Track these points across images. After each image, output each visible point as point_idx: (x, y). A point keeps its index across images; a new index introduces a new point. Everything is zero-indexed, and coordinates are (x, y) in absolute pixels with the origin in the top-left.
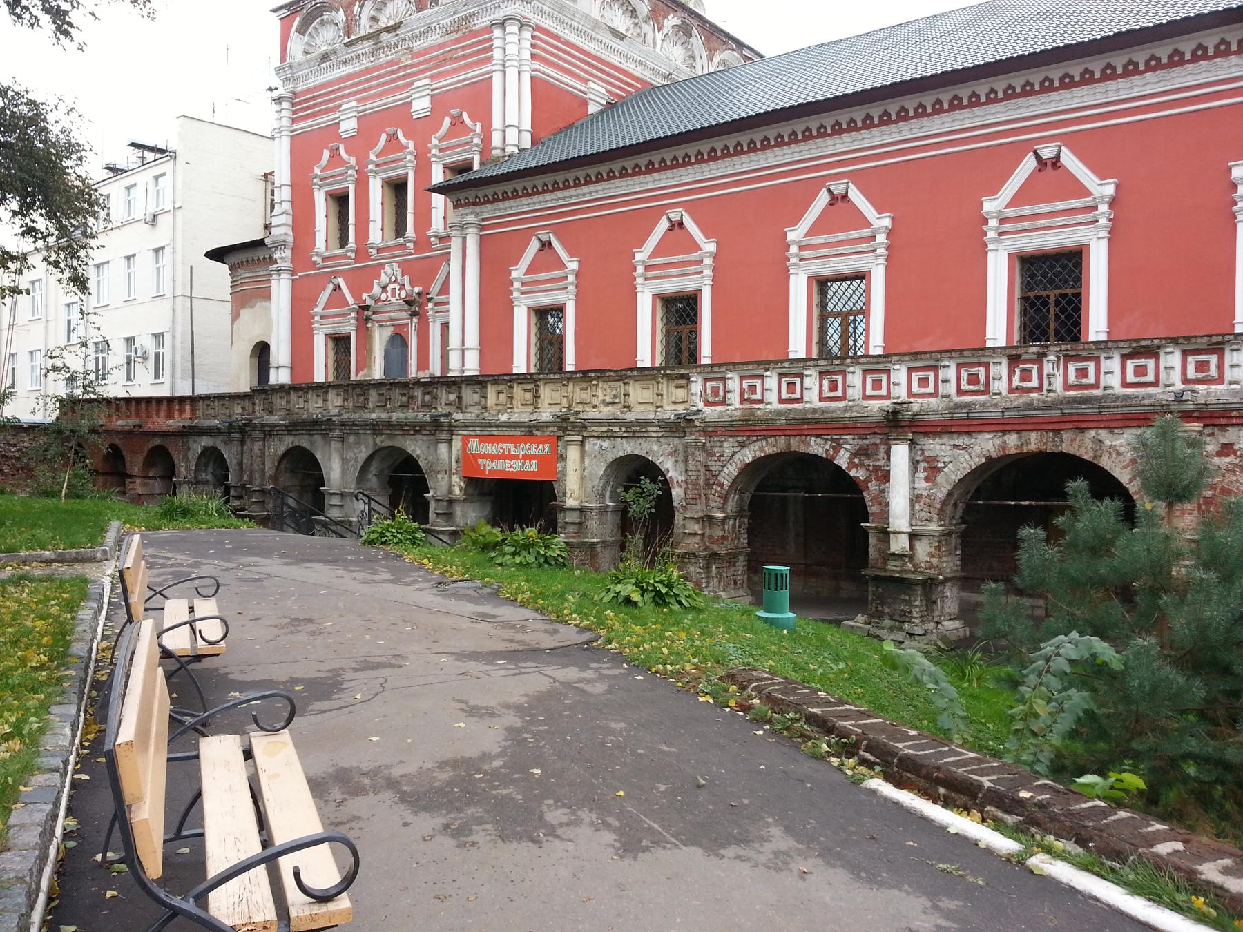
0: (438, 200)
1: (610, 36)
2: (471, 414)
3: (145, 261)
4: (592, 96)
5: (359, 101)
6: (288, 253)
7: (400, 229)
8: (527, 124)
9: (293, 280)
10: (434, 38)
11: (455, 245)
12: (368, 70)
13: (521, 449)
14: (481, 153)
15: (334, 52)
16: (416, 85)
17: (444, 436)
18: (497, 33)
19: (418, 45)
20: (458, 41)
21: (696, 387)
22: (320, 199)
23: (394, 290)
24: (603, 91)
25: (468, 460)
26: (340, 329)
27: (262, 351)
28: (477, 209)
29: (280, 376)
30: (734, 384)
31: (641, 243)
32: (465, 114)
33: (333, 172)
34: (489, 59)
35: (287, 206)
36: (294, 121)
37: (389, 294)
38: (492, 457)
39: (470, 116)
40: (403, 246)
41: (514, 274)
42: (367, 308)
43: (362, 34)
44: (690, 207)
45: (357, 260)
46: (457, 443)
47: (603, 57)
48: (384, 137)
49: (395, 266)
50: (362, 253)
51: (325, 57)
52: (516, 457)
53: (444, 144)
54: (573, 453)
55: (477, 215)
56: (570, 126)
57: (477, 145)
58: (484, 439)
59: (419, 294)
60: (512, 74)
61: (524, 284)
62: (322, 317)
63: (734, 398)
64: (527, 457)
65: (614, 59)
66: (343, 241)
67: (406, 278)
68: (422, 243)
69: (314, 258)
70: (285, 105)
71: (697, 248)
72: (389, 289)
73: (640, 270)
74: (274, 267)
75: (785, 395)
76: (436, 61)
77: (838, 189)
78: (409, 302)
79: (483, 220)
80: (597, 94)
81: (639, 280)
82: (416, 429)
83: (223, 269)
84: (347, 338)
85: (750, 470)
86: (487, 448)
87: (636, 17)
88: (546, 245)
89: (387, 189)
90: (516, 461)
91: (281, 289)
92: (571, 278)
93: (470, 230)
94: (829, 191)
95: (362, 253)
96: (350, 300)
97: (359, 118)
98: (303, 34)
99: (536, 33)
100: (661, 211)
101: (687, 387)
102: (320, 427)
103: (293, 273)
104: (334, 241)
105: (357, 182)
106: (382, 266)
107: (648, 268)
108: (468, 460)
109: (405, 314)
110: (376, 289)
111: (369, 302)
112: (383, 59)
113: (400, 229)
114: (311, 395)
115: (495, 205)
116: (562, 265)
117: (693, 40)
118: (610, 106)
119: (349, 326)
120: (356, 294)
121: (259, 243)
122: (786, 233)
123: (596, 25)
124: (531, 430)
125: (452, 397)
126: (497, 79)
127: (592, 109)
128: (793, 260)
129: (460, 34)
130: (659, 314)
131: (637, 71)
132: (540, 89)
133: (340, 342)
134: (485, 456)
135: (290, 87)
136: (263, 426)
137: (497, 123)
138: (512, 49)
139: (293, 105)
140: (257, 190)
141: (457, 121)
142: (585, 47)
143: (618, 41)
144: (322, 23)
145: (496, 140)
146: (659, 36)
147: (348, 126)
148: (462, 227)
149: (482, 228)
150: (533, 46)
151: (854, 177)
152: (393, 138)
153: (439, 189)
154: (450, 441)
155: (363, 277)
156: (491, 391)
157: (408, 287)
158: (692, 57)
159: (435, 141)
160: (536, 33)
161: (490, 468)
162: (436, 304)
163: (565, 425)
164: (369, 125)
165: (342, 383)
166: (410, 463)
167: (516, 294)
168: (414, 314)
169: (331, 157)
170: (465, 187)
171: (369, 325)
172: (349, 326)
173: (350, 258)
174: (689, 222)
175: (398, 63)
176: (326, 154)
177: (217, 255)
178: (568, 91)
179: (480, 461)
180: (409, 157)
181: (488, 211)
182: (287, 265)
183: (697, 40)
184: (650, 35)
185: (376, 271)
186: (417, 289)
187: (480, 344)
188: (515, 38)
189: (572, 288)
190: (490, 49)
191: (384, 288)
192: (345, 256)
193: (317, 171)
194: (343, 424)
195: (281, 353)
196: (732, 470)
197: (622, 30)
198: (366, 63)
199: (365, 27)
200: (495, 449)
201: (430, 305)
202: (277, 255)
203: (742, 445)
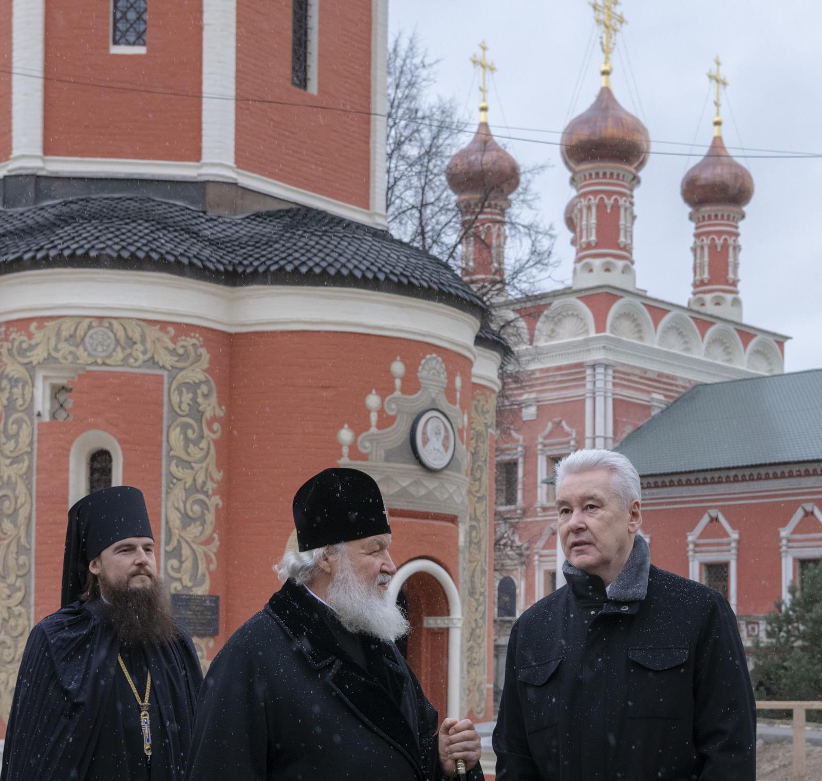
4: (654, 403)
24: (662, 397)
34: (584, 385)
39: (568, 423)
44: (723, 509)
53: (548, 441)
71: (726, 535)
73: (691, 547)
77: (809, 507)
81: (690, 553)
94: (804, 509)
107: (696, 545)
126: (589, 403)
127: (655, 412)
128: (784, 548)
132: (619, 405)
150: (614, 378)
168: (523, 563)
174: (722, 519)
190: (584, 378)
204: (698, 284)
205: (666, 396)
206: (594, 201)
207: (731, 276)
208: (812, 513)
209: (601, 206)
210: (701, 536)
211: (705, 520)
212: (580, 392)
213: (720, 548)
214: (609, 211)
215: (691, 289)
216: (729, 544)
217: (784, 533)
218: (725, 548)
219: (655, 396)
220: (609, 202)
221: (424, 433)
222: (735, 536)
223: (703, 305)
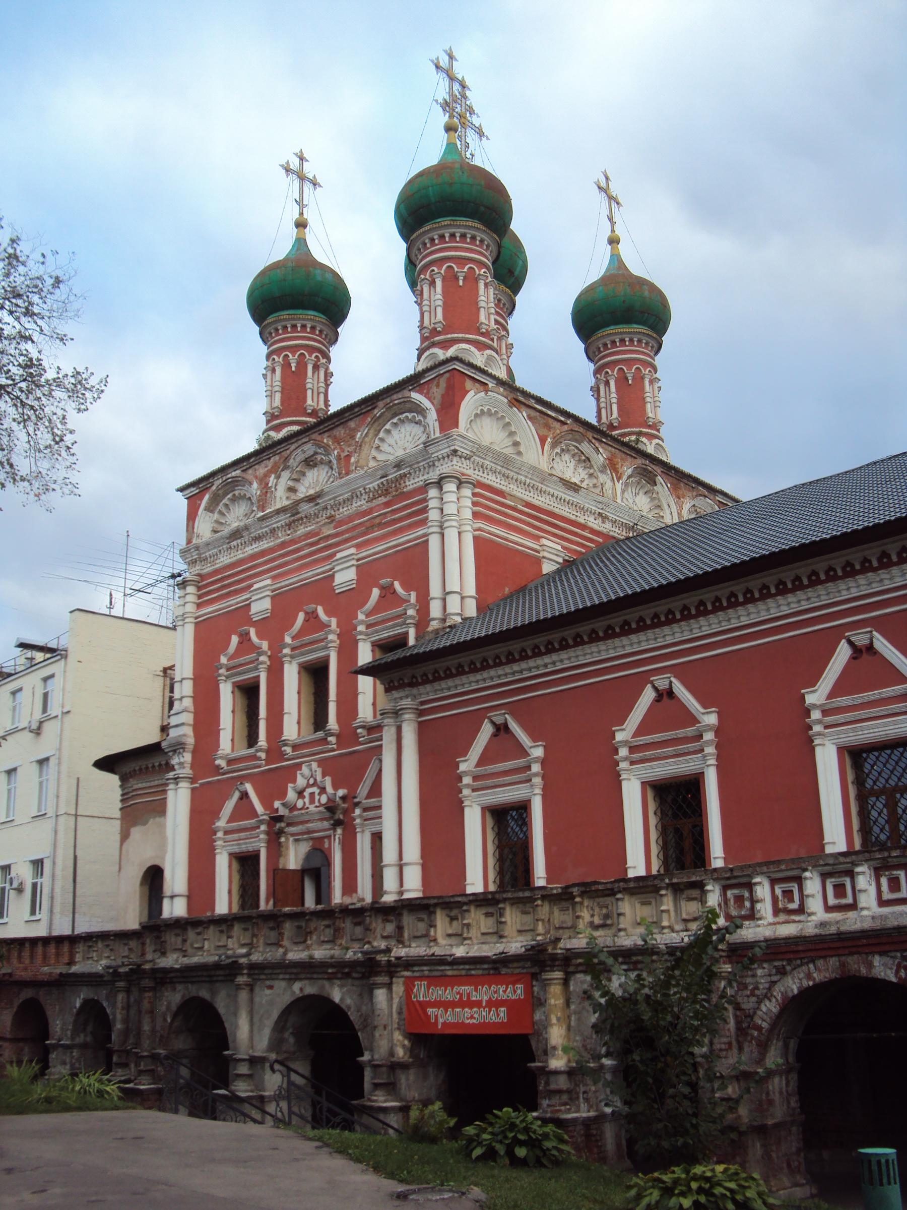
0: (365, 683)
1: (563, 489)
2: (417, 950)
3: (28, 775)
5: (274, 578)
6: (187, 757)
7: (319, 720)
8: (471, 589)
9: (193, 790)
10: (361, 504)
11: (388, 735)
12: (283, 545)
13: (483, 994)
14: (417, 626)
15: (246, 528)
16: (339, 556)
17: (380, 979)
18: (433, 493)
19: (345, 511)
20: (387, 504)
22: (226, 691)
23: (312, 794)
24: (559, 548)
25: (413, 1011)
26: (247, 846)
27: (154, 877)
28: (415, 691)
29: (175, 908)
30: (763, 890)
31: (621, 720)
32: (397, 585)
33: (242, 660)
34: (424, 522)
35: (188, 703)
36: (199, 606)
37: (307, 800)
40: (324, 741)
41: (463, 767)
42: (280, 819)
43: (278, 506)
44: (679, 671)
45: (268, 761)
46: (399, 988)
47: (556, 511)
48: (301, 616)
49: (314, 765)
50: (275, 750)
51: (236, 534)
52: (478, 1004)
53: (372, 619)
54: (555, 996)
55: (414, 697)
56: (522, 589)
57: (411, 617)
59: (344, 798)
60: (451, 535)
61: (475, 778)
62: (226, 833)
63: (765, 908)
64: (493, 1004)
66: (252, 739)
67: (328, 781)
68: (347, 735)
69: (217, 762)
70: (191, 589)
71: (694, 720)
72: (306, 794)
73: (623, 752)
74: (171, 775)
75: (832, 901)
76: (362, 529)
78: (331, 808)
79: (422, 703)
80: (551, 553)
82: (341, 970)
83: (112, 780)
84: (256, 856)
85: (792, 1005)
87: (591, 467)
88: (501, 730)
89: (304, 674)
90: (479, 1009)
91: (179, 801)
92: (536, 768)
93: (407, 716)
95: (275, 750)
96: (259, 808)
97: (273, 598)
98: (212, 512)
99: (477, 490)
102: (225, 972)
103: (193, 780)
104: (242, 741)
105: (269, 670)
106: (299, 766)
107: (633, 749)
108: (413, 1011)
109: (326, 824)
110: (291, 795)
111: (283, 811)
112: (301, 531)
113: (319, 720)
114: (212, 931)
115: (436, 685)
118: (568, 565)
119: (259, 844)
120: (267, 802)
121: (153, 749)
122: (803, 696)
124: (496, 968)
125: (390, 928)
126: (434, 543)
128: (817, 728)
129: (388, 498)
130: (652, 806)
131: (594, 523)
132: (486, 551)
133: (246, 863)
134: (437, 1004)
135: (197, 569)
136: (154, 971)
137: (435, 590)
138: (450, 509)
139: (199, 588)
140: (155, 688)
141: (388, 592)
143: (571, 493)
144: (234, 500)
145: (435, 610)
146: (619, 486)
147: (261, 606)
148: (396, 713)
149: (421, 713)
150: (474, 504)
151: (879, 624)
152: (312, 616)
153: (367, 670)
154: (389, 986)
155: (274, 782)
156: (440, 919)
157: (329, 789)
159: (361, 617)
160: (477, 490)
161: (443, 1019)
162: (365, 810)
164: (286, 605)
165: (247, 916)
166: (336, 1014)
168: (337, 823)
169: (240, 643)
170: (399, 667)
171: (283, 839)
172: (259, 844)
173: (259, 759)
174: (680, 689)
175: (317, 534)
176: (235, 640)
177: (106, 764)
178: (517, 550)
179: (430, 1011)
180: (331, 637)
181: (428, 692)
182: (187, 771)
183: (663, 487)
184: (609, 484)
185: (291, 773)
186: (341, 792)
187: (423, 857)
188: (452, 497)
189: (537, 781)
190: (425, 510)
191: (300, 794)
192: (254, 757)
193: (223, 660)
194: (252, 967)
195: (176, 879)
196: (771, 1007)
198: (282, 537)
199: (281, 499)
200: (448, 994)
201: (358, 811)
202: (175, 761)
203: (782, 972)
208: (870, 648)
209: (450, 279)
210: (641, 730)
212: (421, 531)
214: (461, 283)
217: (815, 697)
218: (691, 746)
219: (544, 541)
220: (462, 272)
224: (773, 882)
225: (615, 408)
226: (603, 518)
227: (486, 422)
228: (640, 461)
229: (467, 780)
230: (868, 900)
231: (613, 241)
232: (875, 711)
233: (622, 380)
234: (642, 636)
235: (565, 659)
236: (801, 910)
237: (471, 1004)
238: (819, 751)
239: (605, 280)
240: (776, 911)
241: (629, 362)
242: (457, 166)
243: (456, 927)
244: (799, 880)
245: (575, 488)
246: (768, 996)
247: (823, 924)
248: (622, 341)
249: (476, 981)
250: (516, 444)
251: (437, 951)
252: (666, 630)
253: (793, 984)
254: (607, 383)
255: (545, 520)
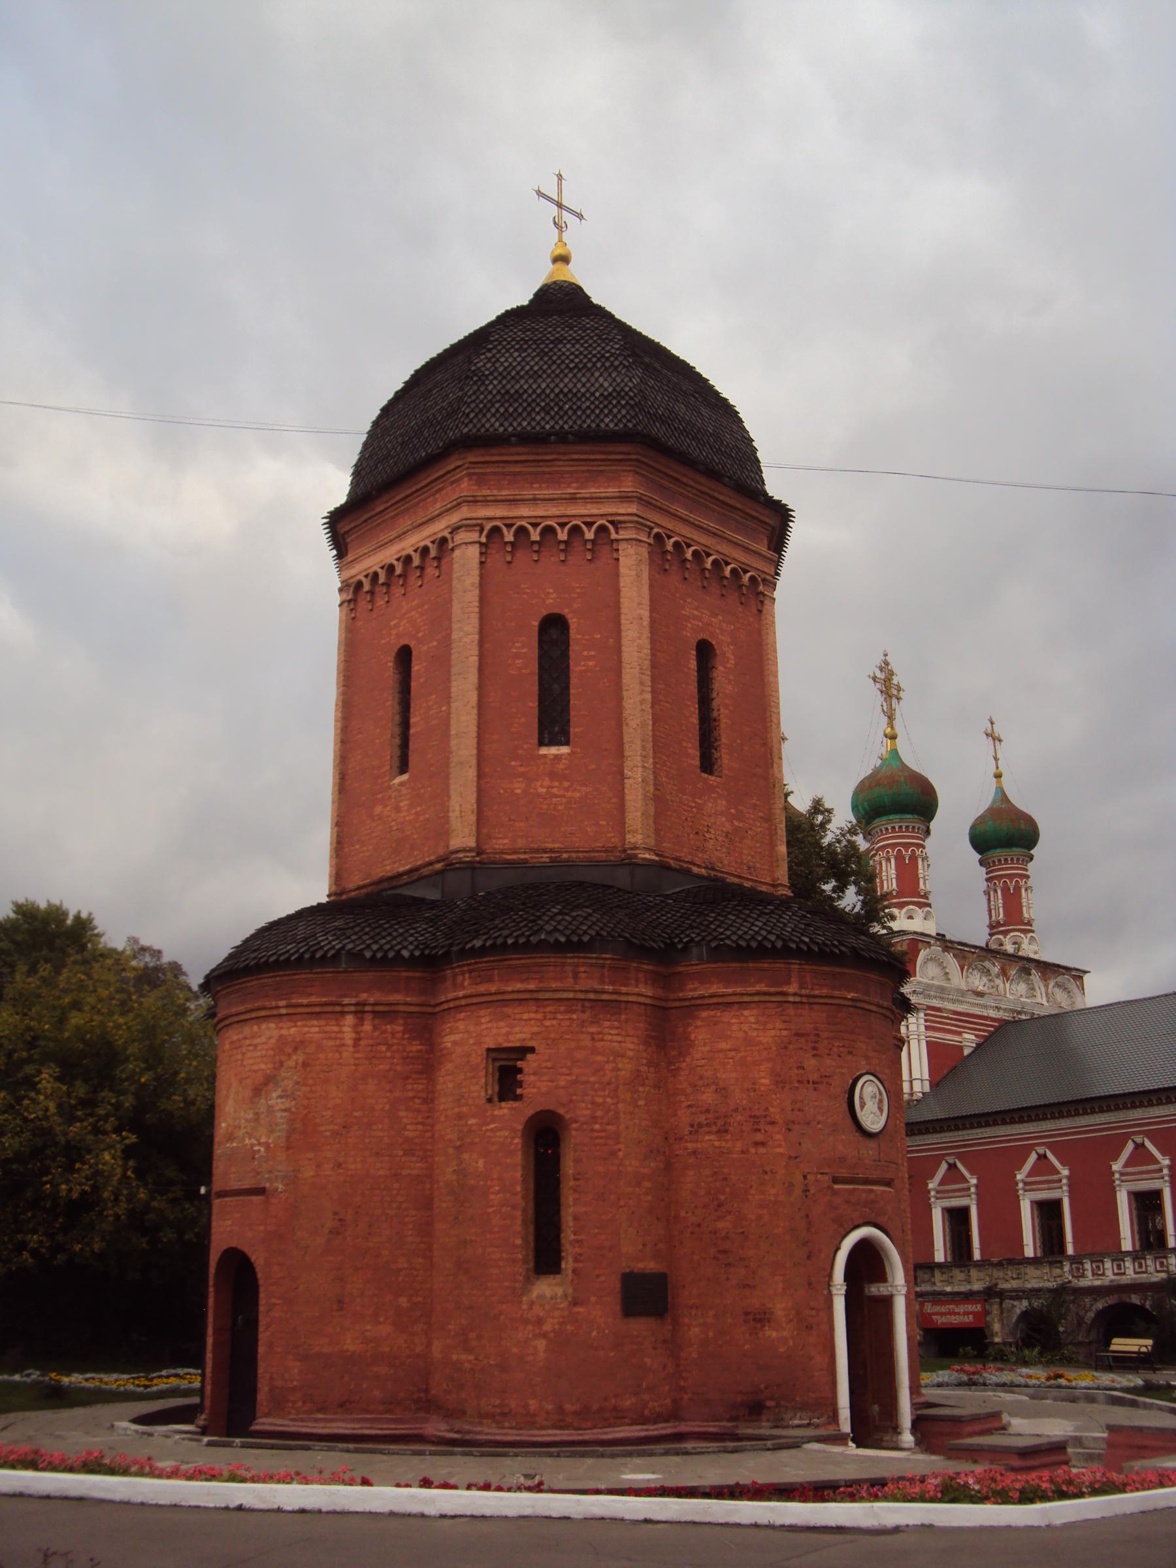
8: (926, 1076)
13: (961, 1308)
21: (1067, 1268)
24: (973, 1037)
30: (1088, 1266)
38: (942, 1314)
41: (931, 1186)
44: (1050, 1146)
52: (958, 1314)
58: (934, 1303)
61: (938, 1192)
63: (1089, 1273)
64: (966, 1313)
65: (976, 1011)
71: (1058, 1172)
73: (1021, 1185)
77: (1138, 1139)
80: (969, 1040)
81: (1021, 1192)
85: (1100, 1314)
86: (938, 1309)
88: (952, 1166)
92: (973, 1190)
100: (1031, 1148)
101: (1062, 1268)
107: (1025, 1183)
116: (965, 1180)
117: (1032, 977)
118: (979, 1046)
123: (963, 993)
124: (968, 1297)
127: (966, 1052)
128: (1117, 1182)
130: (1036, 1213)
131: (992, 1014)
132: (934, 1050)
134: (937, 1314)
142: (959, 1010)
150: (926, 1021)
151: (1147, 1134)
158: (1033, 989)
161: (941, 1321)
163: (991, 1293)
167: (933, 1200)
174: (1050, 1155)
183: (1035, 976)
184: (1001, 986)
196: (1091, 1315)
197: (981, 988)
200: (943, 1309)
203: (1096, 1300)
204: (994, 927)
205: (976, 1036)
206: (893, 853)
207: (1026, 915)
208: (1143, 1144)
209: (899, 858)
210: (1029, 1175)
211: (1033, 1157)
213: (1052, 1185)
215: (988, 931)
216: (1060, 1181)
217: (1116, 1166)
218: (1056, 1185)
219: (965, 1036)
220: (907, 854)
221: (861, 1098)
222: (1065, 1172)
223: (1001, 945)
224: (1092, 1262)
225: (1001, 910)
226: (998, 1009)
227: (930, 964)
228: (1020, 964)
229: (933, 1193)
230: (1130, 1272)
231: (998, 776)
232: (1144, 1176)
233: (1005, 889)
234: (1030, 1124)
235: (988, 1132)
236: (1103, 1274)
237: (955, 1314)
238: (1118, 1194)
239: (993, 812)
240: (1093, 1274)
241: (1011, 877)
242: (902, 779)
243: (945, 1277)
244: (1102, 1262)
245: (980, 994)
246: (1090, 1309)
247: (1112, 1281)
248: (1006, 860)
249: (957, 1303)
250: (947, 974)
251: (936, 1288)
252: (1043, 1123)
253: (1100, 1305)
254: (995, 891)
255: (965, 1020)
